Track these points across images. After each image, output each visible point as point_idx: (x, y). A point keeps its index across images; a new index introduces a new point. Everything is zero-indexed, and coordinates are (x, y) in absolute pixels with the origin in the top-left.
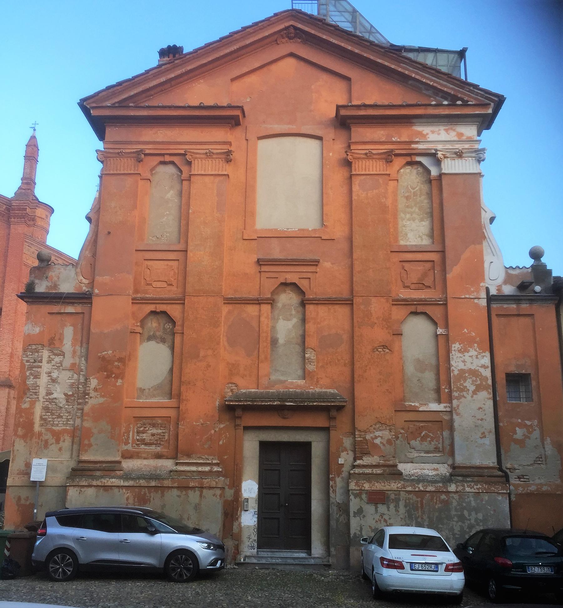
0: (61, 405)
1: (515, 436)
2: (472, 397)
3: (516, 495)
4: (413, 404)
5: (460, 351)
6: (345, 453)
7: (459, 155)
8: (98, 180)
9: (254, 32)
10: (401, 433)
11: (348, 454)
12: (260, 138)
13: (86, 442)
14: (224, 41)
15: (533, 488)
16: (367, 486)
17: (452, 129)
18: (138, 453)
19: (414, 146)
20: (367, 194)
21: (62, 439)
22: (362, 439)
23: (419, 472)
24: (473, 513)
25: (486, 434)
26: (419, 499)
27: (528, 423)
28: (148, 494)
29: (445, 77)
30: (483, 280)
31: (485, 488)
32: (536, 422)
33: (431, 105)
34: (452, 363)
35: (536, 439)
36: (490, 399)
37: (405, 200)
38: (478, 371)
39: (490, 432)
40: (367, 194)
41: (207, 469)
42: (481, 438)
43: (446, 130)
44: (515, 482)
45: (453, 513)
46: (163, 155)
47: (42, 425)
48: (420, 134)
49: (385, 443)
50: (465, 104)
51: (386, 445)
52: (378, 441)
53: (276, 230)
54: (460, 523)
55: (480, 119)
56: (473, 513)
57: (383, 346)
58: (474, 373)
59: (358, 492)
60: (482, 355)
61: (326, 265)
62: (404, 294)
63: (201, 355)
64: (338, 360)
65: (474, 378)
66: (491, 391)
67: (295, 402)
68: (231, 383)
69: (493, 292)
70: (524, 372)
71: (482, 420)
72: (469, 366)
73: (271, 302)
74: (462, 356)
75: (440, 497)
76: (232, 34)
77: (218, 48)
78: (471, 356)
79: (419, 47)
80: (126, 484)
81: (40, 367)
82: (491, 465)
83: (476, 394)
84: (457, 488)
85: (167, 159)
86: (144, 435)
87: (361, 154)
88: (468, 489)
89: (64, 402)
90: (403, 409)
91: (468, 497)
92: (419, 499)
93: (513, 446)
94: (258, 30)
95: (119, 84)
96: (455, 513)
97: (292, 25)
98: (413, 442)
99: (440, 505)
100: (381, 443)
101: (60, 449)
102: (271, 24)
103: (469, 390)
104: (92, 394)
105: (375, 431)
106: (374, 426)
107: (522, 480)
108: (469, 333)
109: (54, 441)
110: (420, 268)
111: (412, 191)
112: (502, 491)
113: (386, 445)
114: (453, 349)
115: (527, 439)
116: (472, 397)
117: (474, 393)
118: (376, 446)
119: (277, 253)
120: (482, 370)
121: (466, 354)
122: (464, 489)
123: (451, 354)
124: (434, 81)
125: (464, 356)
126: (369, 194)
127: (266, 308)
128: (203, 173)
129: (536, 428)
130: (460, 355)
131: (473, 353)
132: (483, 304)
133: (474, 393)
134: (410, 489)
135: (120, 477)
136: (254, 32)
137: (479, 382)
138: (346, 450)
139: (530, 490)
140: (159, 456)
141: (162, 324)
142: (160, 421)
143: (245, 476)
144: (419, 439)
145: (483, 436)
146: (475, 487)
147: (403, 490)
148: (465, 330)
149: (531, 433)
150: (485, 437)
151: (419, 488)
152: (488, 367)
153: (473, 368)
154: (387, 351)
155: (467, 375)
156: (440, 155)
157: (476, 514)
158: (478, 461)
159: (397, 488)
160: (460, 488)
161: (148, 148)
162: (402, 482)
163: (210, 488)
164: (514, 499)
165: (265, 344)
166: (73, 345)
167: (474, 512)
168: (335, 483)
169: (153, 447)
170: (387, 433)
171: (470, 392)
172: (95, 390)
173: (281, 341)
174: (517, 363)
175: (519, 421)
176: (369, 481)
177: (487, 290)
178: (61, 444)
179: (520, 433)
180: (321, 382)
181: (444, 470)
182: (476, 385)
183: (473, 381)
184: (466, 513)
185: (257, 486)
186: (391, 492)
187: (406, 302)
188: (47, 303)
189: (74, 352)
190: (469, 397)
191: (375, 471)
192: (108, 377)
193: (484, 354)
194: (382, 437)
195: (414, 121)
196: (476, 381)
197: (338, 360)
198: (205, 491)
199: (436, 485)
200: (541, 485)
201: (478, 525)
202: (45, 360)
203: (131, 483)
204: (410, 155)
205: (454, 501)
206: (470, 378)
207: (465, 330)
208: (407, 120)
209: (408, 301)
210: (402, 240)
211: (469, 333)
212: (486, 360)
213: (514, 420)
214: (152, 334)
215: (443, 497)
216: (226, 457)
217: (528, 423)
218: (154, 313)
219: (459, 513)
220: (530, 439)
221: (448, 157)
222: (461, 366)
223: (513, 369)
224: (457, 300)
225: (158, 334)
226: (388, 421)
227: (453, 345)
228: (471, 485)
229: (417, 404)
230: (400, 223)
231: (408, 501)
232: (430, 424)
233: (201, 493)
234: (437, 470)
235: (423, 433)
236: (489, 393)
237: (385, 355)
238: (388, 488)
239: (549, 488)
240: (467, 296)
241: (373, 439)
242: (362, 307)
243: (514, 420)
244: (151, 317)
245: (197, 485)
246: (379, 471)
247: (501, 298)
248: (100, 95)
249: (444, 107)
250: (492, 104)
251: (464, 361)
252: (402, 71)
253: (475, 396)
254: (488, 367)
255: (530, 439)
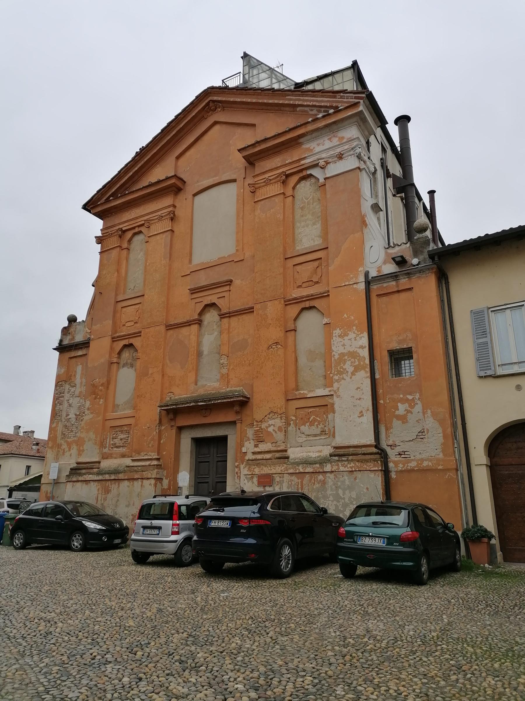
0: (73, 423)
1: (397, 413)
2: (351, 378)
3: (396, 472)
4: (302, 392)
5: (340, 336)
6: (248, 442)
7: (340, 157)
8: (98, 256)
9: (184, 117)
10: (292, 420)
11: (250, 443)
12: (195, 195)
13: (81, 448)
14: (165, 131)
15: (413, 464)
16: (257, 471)
17: (334, 136)
18: (112, 454)
19: (302, 162)
20: (266, 215)
21: (72, 448)
22: (259, 428)
23: (304, 455)
24: (347, 492)
25: (364, 412)
26: (300, 481)
27: (410, 397)
28: (110, 486)
29: (320, 94)
30: (362, 264)
31: (358, 466)
32: (417, 396)
33: (308, 122)
34: (333, 348)
35: (419, 412)
36: (367, 377)
37: (300, 211)
38: (356, 352)
39: (368, 410)
40: (266, 215)
41: (147, 463)
42: (359, 417)
43: (330, 139)
44: (396, 459)
45: (329, 492)
46: (134, 228)
47: (62, 438)
48: (309, 150)
49: (276, 430)
50: (337, 111)
51: (278, 432)
52: (270, 429)
53: (203, 263)
54: (335, 503)
55: (355, 119)
56: (347, 492)
57: (276, 343)
58: (353, 355)
59: (250, 476)
60: (360, 336)
61: (237, 282)
62: (296, 293)
63: (150, 372)
64: (245, 361)
65: (353, 360)
66: (368, 370)
67: (205, 401)
68: (170, 392)
69: (373, 273)
70: (405, 346)
71: (360, 399)
72: (348, 349)
73: (199, 322)
74: (342, 340)
75: (317, 477)
76: (169, 124)
77: (162, 138)
78: (350, 339)
79: (318, 77)
80: (97, 478)
81: (63, 397)
82: (369, 443)
83: (355, 375)
84: (332, 468)
85: (137, 230)
86: (116, 440)
87: (261, 183)
88: (342, 469)
89: (74, 420)
90: (294, 398)
91: (343, 476)
92: (300, 481)
93: (396, 423)
94: (187, 114)
95: (104, 187)
96: (331, 492)
97: (210, 100)
98: (302, 428)
99: (317, 485)
100: (274, 430)
101: (71, 455)
102: (195, 106)
103: (347, 372)
104: (87, 412)
105: (269, 420)
106: (268, 416)
107: (403, 456)
108: (349, 317)
109: (67, 449)
110: (311, 266)
111: (306, 201)
112: (374, 469)
113: (278, 432)
114: (334, 335)
115: (409, 414)
116: (351, 378)
117: (353, 374)
118: (269, 433)
119: (203, 280)
120: (360, 351)
121: (346, 338)
122: (339, 468)
123: (332, 340)
124: (314, 101)
125: (344, 340)
126: (268, 214)
127: (195, 327)
128: (156, 233)
129: (419, 402)
130: (341, 340)
131: (352, 335)
132: (362, 288)
133: (353, 374)
134: (291, 471)
135: (98, 474)
136: (184, 117)
137: (357, 363)
138: (249, 439)
139: (410, 467)
140: (123, 456)
141: (131, 354)
142: (126, 429)
143: (181, 468)
144: (308, 424)
145: (361, 415)
146: (349, 466)
147: (286, 472)
148: (345, 315)
149: (413, 407)
150: (362, 415)
151: (299, 470)
152: (365, 347)
153: (351, 350)
154: (279, 346)
155: (346, 357)
156: (322, 163)
157: (350, 493)
158: (357, 440)
159: (281, 470)
160: (335, 468)
161: (124, 227)
162: (285, 465)
163: (148, 479)
164: (395, 477)
165: (193, 357)
166: (81, 378)
167: (348, 491)
168: (240, 470)
169: (121, 449)
170: (279, 421)
171: (350, 373)
172: (88, 409)
173: (205, 353)
174: (399, 338)
175: (401, 396)
176: (258, 465)
177: (367, 274)
178: (72, 451)
179: (402, 408)
180: (232, 382)
181: (327, 451)
182: (354, 366)
183: (352, 362)
184: (340, 492)
185: (189, 476)
186: (277, 475)
187: (297, 301)
188: (68, 351)
189: (81, 383)
190: (348, 379)
191: (268, 456)
192: (95, 398)
193: (362, 335)
194: (274, 425)
195: (301, 140)
196: (355, 362)
197: (245, 361)
198: (144, 481)
199: (314, 466)
200: (422, 460)
201: (352, 503)
202: (66, 391)
203: (100, 477)
204: (301, 171)
205: (330, 480)
206: (350, 360)
207: (345, 315)
208: (294, 143)
209: (298, 299)
210: (298, 246)
211: (349, 317)
212: (364, 341)
213: (396, 396)
214: (125, 362)
215: (321, 477)
216: (164, 453)
217: (410, 397)
218: (125, 346)
219: (335, 492)
220: (412, 413)
221: (330, 163)
222: (341, 350)
223: (395, 346)
224: (340, 288)
225: (129, 361)
226: (279, 410)
227: (334, 332)
228: (344, 464)
229: (305, 392)
230: (297, 231)
231: (290, 483)
232: (317, 409)
233: (142, 482)
234: (320, 451)
235: (312, 418)
236: (366, 372)
237: (277, 350)
238: (273, 471)
239: (430, 464)
240: (347, 283)
241: (267, 427)
242: (260, 312)
243: (396, 396)
244: (125, 349)
245: (139, 477)
246: (268, 456)
247: (382, 278)
248: (94, 198)
249: (321, 120)
250: (361, 101)
251: (344, 345)
252: (288, 103)
253: (353, 377)
254: (365, 347)
255: (412, 413)
